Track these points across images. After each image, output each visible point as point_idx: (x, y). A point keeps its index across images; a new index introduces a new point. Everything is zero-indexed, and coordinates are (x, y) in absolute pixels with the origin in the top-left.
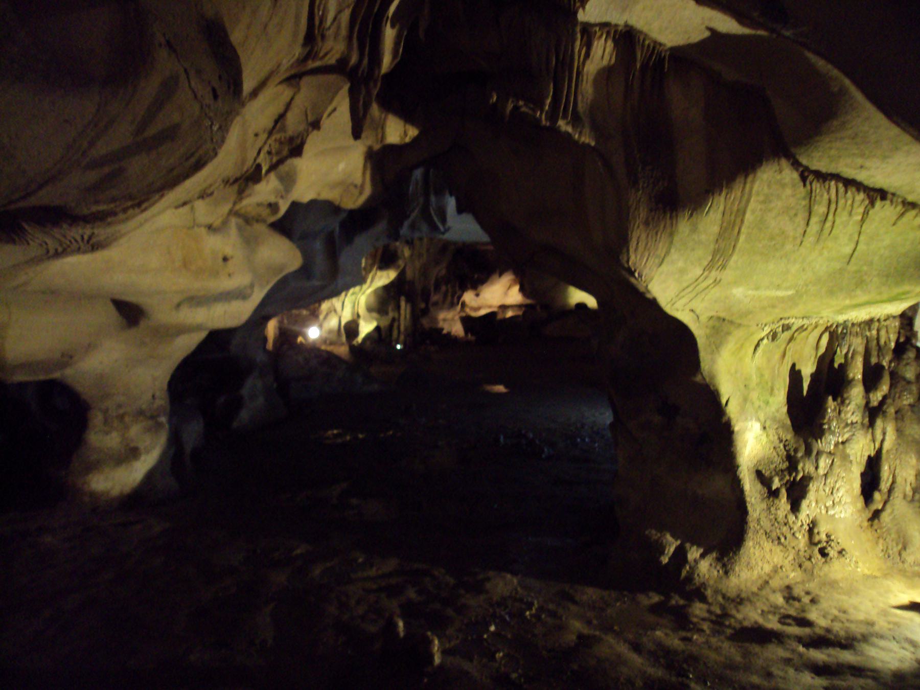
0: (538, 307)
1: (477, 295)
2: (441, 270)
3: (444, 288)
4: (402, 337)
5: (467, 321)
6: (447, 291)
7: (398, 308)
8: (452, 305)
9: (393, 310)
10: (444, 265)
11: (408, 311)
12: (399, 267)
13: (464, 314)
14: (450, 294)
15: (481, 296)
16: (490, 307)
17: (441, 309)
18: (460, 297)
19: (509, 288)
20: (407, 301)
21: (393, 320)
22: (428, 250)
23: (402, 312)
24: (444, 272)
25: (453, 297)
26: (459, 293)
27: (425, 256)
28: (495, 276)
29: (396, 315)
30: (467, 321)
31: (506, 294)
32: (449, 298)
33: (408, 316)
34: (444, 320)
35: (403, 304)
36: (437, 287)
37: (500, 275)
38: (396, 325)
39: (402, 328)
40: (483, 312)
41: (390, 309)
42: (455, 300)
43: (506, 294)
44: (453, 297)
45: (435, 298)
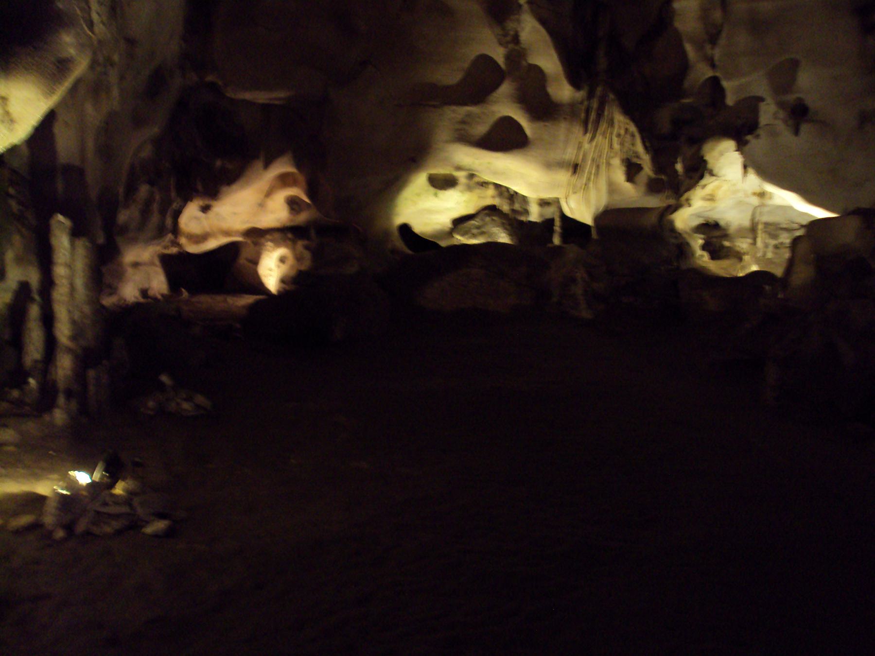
0: (313, 232)
1: (205, 209)
2: (138, 145)
3: (144, 190)
4: (64, 365)
5: (178, 266)
6: (148, 203)
7: (44, 257)
8: (161, 232)
9: (20, 260)
10: (154, 130)
11: (80, 264)
12: (63, 66)
13: (174, 250)
14: (155, 207)
15: (211, 214)
16: (227, 233)
17: (134, 241)
18: (177, 214)
19: (269, 194)
20: (76, 233)
21: (24, 288)
22: (122, 78)
23: (60, 271)
24: (147, 152)
25: (163, 212)
26: (175, 206)
27: (115, 92)
28: (259, 164)
29: (34, 277)
30: (178, 266)
31: (262, 205)
32: (155, 219)
33: (79, 282)
34: (136, 265)
35: (62, 242)
36: (131, 189)
37: (267, 165)
38: (34, 311)
39: (63, 331)
40: (212, 244)
41: (10, 255)
42: (169, 221)
43: (262, 205)
44: (163, 212)
45: (123, 217)
